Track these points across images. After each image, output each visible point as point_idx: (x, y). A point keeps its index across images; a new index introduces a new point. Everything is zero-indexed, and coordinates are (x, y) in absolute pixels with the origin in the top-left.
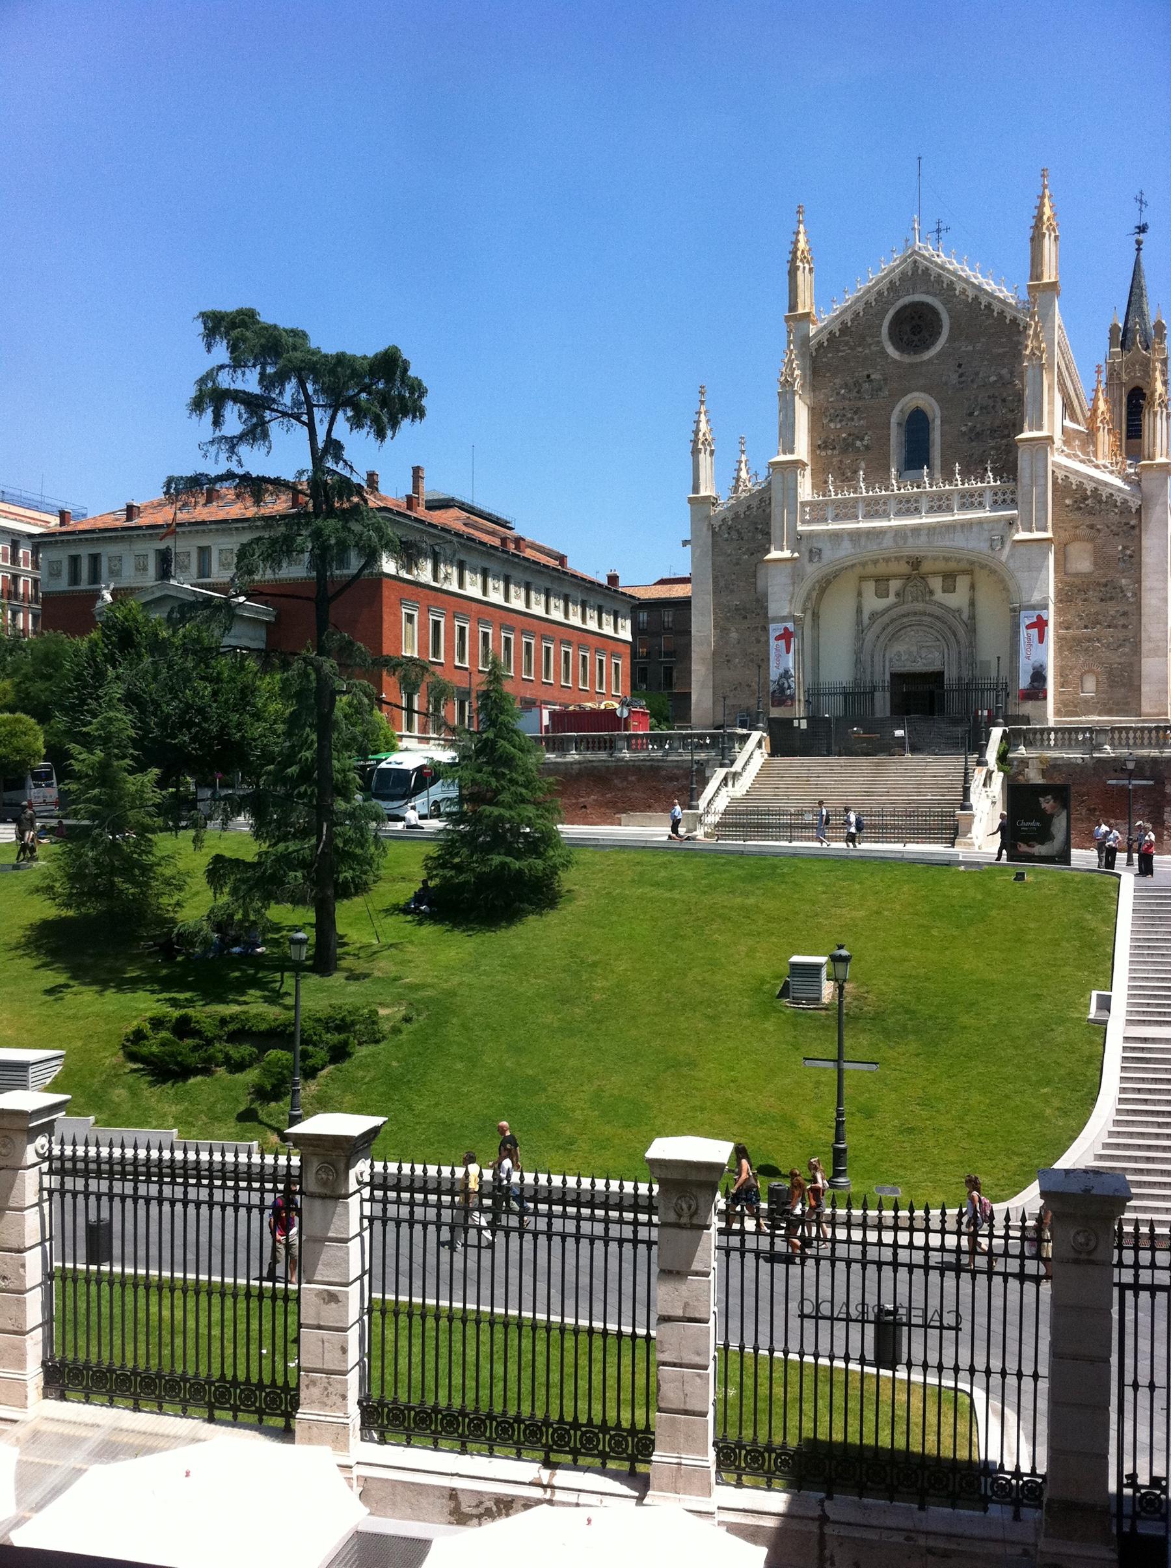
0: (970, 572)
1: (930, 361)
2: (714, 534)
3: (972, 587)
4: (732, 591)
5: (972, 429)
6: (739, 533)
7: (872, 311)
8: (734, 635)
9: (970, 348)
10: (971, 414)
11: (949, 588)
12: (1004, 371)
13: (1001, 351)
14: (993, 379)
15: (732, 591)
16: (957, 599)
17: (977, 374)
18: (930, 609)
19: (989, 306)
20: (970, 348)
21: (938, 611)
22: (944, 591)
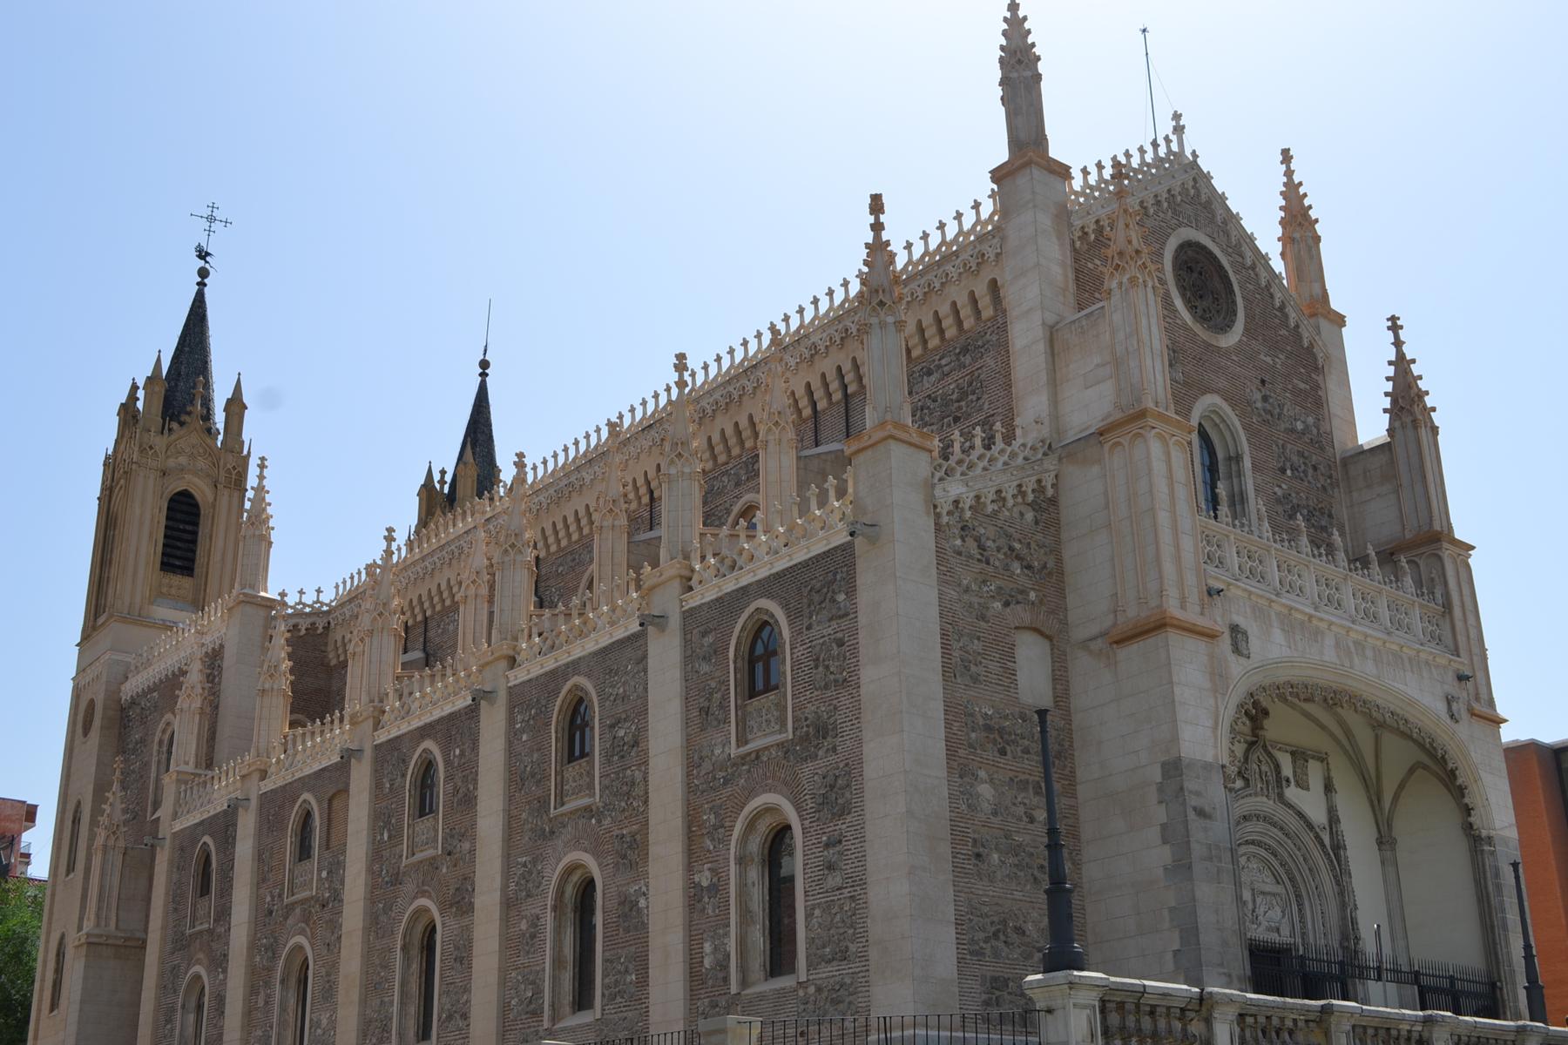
0: (1322, 759)
1: (1226, 353)
2: (938, 528)
3: (1329, 788)
4: (975, 679)
5: (1287, 496)
6: (982, 548)
7: (1149, 223)
8: (985, 790)
9: (1268, 359)
10: (1283, 471)
11: (1303, 785)
12: (1310, 420)
13: (1302, 386)
14: (1300, 426)
15: (975, 679)
16: (1312, 804)
17: (1281, 406)
18: (1281, 813)
19: (1282, 308)
20: (1268, 359)
21: (1294, 824)
22: (1298, 785)
